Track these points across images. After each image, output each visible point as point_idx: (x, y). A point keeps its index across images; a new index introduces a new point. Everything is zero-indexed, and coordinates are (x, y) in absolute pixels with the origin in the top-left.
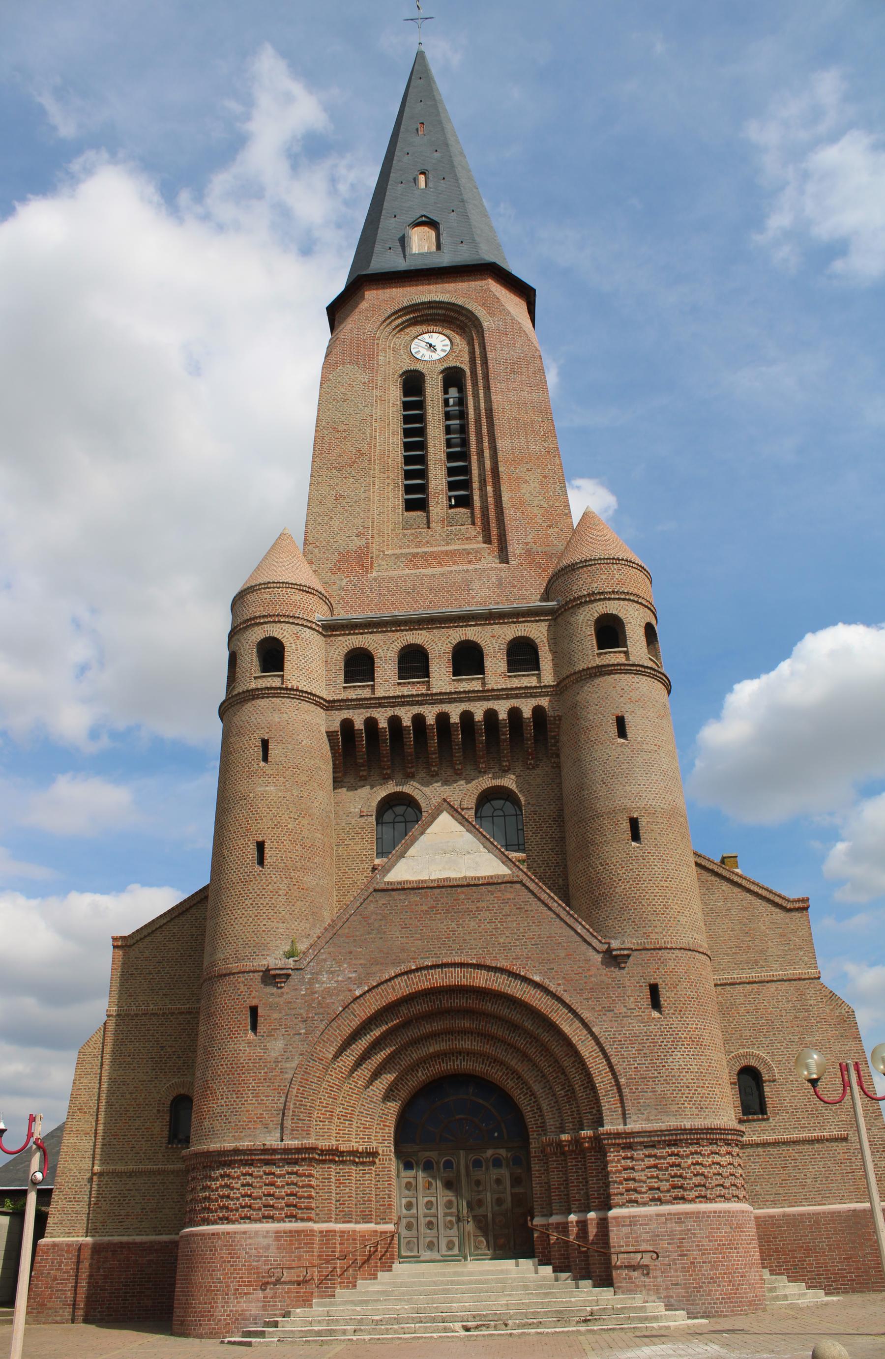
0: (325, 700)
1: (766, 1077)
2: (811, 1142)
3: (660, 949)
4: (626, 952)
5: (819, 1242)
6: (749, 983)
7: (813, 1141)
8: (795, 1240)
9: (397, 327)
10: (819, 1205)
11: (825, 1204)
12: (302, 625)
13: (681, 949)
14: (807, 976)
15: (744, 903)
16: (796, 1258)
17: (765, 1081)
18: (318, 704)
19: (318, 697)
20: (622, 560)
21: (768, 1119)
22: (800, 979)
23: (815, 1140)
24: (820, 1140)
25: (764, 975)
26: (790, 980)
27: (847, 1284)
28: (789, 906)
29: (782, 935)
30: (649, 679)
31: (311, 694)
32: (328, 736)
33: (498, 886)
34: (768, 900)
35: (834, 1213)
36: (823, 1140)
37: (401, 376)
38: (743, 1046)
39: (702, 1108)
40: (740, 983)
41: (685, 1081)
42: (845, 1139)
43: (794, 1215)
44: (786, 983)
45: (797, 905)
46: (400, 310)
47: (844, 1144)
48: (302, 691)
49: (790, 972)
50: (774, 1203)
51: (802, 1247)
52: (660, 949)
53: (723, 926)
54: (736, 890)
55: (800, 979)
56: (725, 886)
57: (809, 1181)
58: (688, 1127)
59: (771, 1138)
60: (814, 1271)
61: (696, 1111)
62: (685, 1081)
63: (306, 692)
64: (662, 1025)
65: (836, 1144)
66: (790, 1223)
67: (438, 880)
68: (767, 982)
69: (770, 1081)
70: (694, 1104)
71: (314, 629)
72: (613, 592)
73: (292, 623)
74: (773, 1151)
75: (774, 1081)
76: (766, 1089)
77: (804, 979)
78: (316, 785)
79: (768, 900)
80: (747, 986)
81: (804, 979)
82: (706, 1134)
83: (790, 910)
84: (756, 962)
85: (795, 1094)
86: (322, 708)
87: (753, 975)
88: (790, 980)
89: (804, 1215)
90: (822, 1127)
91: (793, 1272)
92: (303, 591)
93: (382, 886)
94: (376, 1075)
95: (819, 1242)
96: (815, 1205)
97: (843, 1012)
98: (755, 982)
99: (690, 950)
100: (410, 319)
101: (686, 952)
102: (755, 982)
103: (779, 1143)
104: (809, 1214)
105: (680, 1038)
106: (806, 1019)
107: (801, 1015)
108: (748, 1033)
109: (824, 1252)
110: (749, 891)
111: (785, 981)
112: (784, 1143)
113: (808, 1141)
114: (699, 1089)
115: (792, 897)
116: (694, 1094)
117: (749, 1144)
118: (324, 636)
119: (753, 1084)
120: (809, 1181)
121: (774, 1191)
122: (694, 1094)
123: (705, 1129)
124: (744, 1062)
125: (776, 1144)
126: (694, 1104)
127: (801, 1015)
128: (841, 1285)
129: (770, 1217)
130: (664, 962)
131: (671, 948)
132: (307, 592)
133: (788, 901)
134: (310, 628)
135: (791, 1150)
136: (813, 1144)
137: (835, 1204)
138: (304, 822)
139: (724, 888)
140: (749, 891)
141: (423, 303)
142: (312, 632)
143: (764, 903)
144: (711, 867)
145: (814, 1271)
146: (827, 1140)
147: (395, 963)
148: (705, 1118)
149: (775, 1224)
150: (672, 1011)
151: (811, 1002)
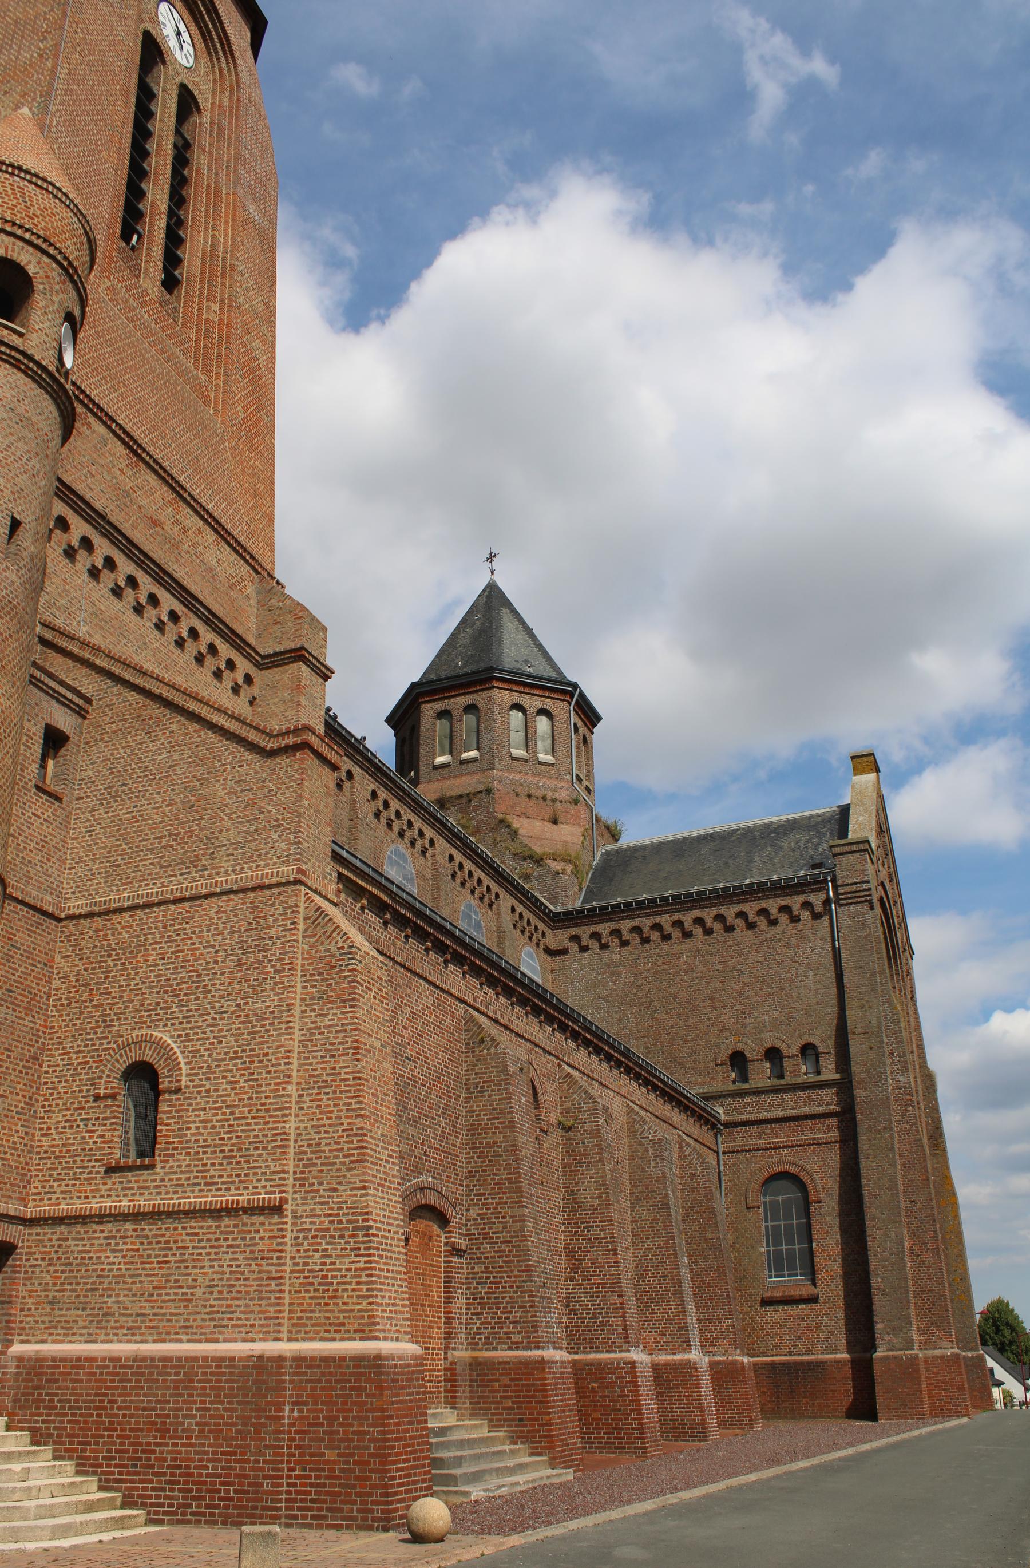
1: (164, 1084)
2: (217, 1213)
5: (185, 1417)
8: (145, 1409)
10: (208, 1341)
11: (217, 1341)
14: (274, 880)
16: (140, 1444)
17: (164, 1092)
21: (152, 1166)
22: (262, 887)
23: (221, 1210)
24: (231, 1211)
25: (203, 886)
26: (244, 890)
27: (218, 1507)
28: (271, 744)
29: (251, 804)
35: (222, 1359)
36: (237, 1210)
38: (141, 1024)
42: (277, 1209)
43: (153, 1359)
44: (236, 898)
45: (283, 743)
47: (276, 1219)
49: (250, 875)
50: (133, 1333)
51: (154, 1423)
53: (158, 798)
54: (193, 727)
55: (262, 887)
56: (177, 724)
57: (199, 1292)
59: (144, 1202)
60: (164, 1474)
66: (142, 1374)
68: (207, 896)
69: (170, 1092)
74: (149, 1229)
75: (178, 1090)
76: (163, 1107)
77: (270, 887)
80: (172, 907)
81: (270, 887)
83: (272, 753)
84: (195, 861)
85: (209, 1117)
87: (185, 885)
88: (244, 890)
89: (170, 1359)
90: (243, 1183)
91: (129, 1473)
95: (185, 1417)
96: (200, 1341)
97: (333, 948)
98: (183, 900)
102: (183, 900)
103: (160, 1213)
104: (205, 1359)
106: (257, 965)
108: (152, 999)
109: (189, 1438)
110: (212, 726)
111: (236, 892)
112: (169, 1214)
113: (211, 1211)
115: (275, 726)
117: (110, 1215)
119: (153, 1098)
120: (199, 1292)
121: (136, 1308)
124: (134, 1056)
125: (156, 1215)
128: (207, 1506)
129: (113, 1359)
133: (270, 735)
135: (170, 1229)
136: (220, 1218)
137: (235, 1340)
139: (173, 727)
140: (212, 726)
143: (233, 746)
144: (158, 691)
145: (164, 1474)
146: (245, 1210)
149: (118, 1374)
151: (272, 932)
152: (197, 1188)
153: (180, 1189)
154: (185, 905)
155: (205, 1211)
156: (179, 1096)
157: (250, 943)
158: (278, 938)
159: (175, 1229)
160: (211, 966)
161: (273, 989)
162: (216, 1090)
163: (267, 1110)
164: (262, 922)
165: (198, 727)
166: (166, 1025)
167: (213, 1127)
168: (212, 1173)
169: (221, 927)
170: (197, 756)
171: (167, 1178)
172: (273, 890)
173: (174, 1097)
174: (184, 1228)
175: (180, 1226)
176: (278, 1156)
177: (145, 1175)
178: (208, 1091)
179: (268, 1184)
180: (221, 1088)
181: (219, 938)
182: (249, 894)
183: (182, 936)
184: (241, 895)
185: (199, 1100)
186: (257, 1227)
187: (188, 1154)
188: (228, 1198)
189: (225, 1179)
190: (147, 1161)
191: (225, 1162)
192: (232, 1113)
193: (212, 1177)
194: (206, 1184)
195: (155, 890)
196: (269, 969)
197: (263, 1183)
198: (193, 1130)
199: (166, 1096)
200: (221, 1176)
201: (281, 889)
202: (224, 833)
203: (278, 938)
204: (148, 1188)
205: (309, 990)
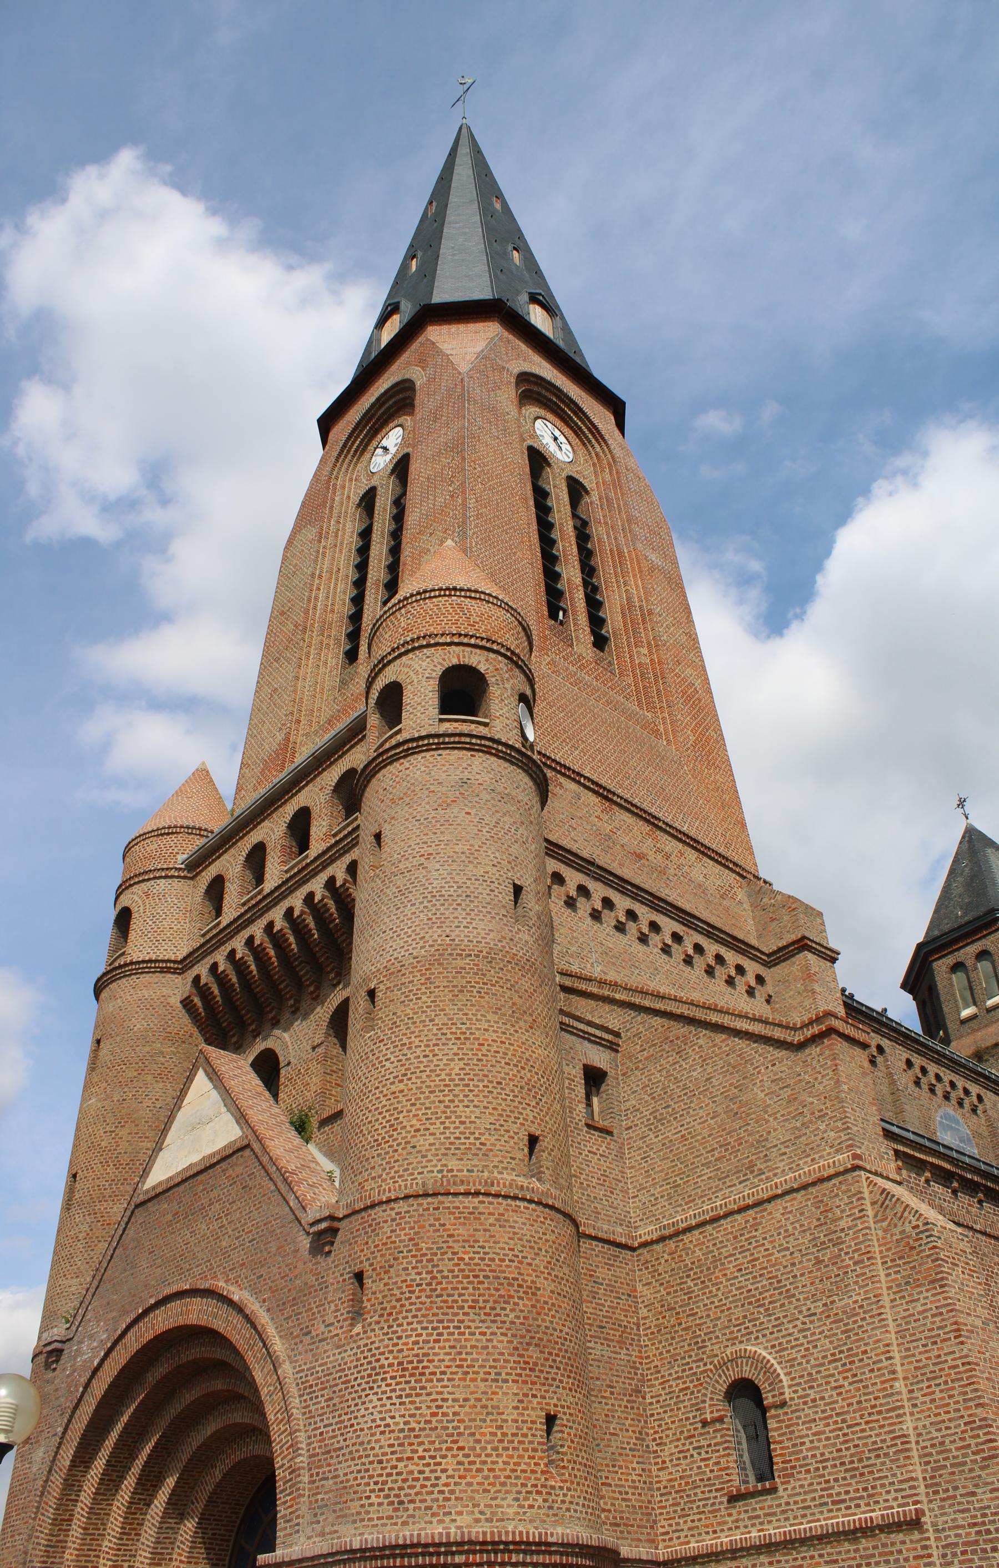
0: (175, 962)
1: (768, 1400)
3: (373, 1206)
4: (323, 1225)
6: (741, 1210)
7: (855, 1531)
9: (356, 451)
12: (155, 878)
13: (407, 1197)
15: (732, 1059)
17: (770, 1408)
18: (168, 970)
19: (163, 961)
20: (412, 595)
21: (774, 1490)
22: (821, 1180)
26: (805, 1187)
28: (798, 1038)
29: (792, 1100)
30: (428, 755)
31: (150, 961)
32: (184, 1006)
33: (230, 1160)
34: (768, 1040)
36: (872, 1529)
37: (359, 505)
39: (401, 1503)
40: (726, 1216)
41: (377, 1450)
42: (915, 1524)
44: (798, 1196)
45: (809, 1033)
46: (354, 430)
47: (916, 1535)
48: (138, 962)
49: (807, 1170)
52: (373, 1206)
53: (701, 1113)
55: (821, 1180)
56: (703, 1038)
58: (356, 1545)
59: (775, 1531)
61: (387, 1510)
62: (377, 1450)
63: (143, 962)
64: (359, 1347)
65: (901, 1536)
67: (178, 1174)
68: (769, 1200)
69: (776, 1407)
70: (387, 1496)
71: (172, 877)
72: (393, 650)
73: (144, 881)
75: (783, 1404)
76: (772, 1424)
77: (829, 1178)
78: (149, 1078)
79: (768, 1040)
80: (738, 1217)
81: (829, 1178)
82: (394, 1556)
83: (801, 1046)
84: (751, 1166)
85: (821, 1428)
86: (174, 973)
88: (805, 1187)
92: (162, 835)
93: (142, 1198)
94: (148, 1484)
97: (908, 1228)
98: (748, 1207)
99: (426, 1195)
100: (368, 432)
101: (420, 1200)
102: (748, 1207)
103: (792, 1541)
105: (382, 1366)
107: (826, 1256)
108: (738, 1313)
110: (737, 1033)
111: (798, 1190)
114: (401, 1465)
116: (389, 1475)
117: (742, 1549)
118: (192, 878)
122: (389, 1475)
123: (385, 1547)
126: (387, 1496)
127: (826, 1256)
130: (375, 1228)
131: (389, 1201)
132: (168, 834)
133: (795, 1029)
134: (166, 877)
136: (856, 1540)
138: (123, 1132)
139: (701, 1042)
140: (737, 1033)
141: (373, 405)
142: (170, 881)
143: (761, 1048)
144: (679, 1011)
146: (881, 1528)
147: (124, 1312)
148: (405, 1523)
150: (376, 1318)
151: (842, 1224)
152: (825, 1509)
153: (808, 1512)
154: (751, 1212)
155: (838, 1533)
156: (785, 1409)
157: (822, 1239)
158: (849, 1228)
159: (812, 1557)
160: (789, 1269)
161: (856, 1283)
162: (822, 1398)
163: (880, 1412)
164: (830, 1215)
165: (724, 1036)
166: (757, 1338)
167: (828, 1439)
168: (837, 1489)
169: (790, 1228)
170: (729, 1064)
171: (791, 1501)
172: (833, 1181)
173: (780, 1411)
174: (821, 1556)
175: (816, 1554)
176: (902, 1462)
177: (769, 1500)
178: (814, 1400)
179: (899, 1495)
180: (826, 1395)
181: (791, 1239)
182: (810, 1189)
183: (754, 1244)
184: (803, 1192)
185: (807, 1411)
186: (898, 1546)
187: (808, 1471)
188: (860, 1516)
189: (852, 1495)
190: (767, 1485)
191: (848, 1475)
192: (844, 1421)
193: (838, 1494)
194: (834, 1503)
195: (719, 1203)
196: (848, 1262)
197: (893, 1494)
198: (808, 1445)
199: (773, 1412)
200: (847, 1492)
201: (841, 1178)
202: (773, 1134)
203: (849, 1228)
204: (774, 1514)
205: (893, 1276)
